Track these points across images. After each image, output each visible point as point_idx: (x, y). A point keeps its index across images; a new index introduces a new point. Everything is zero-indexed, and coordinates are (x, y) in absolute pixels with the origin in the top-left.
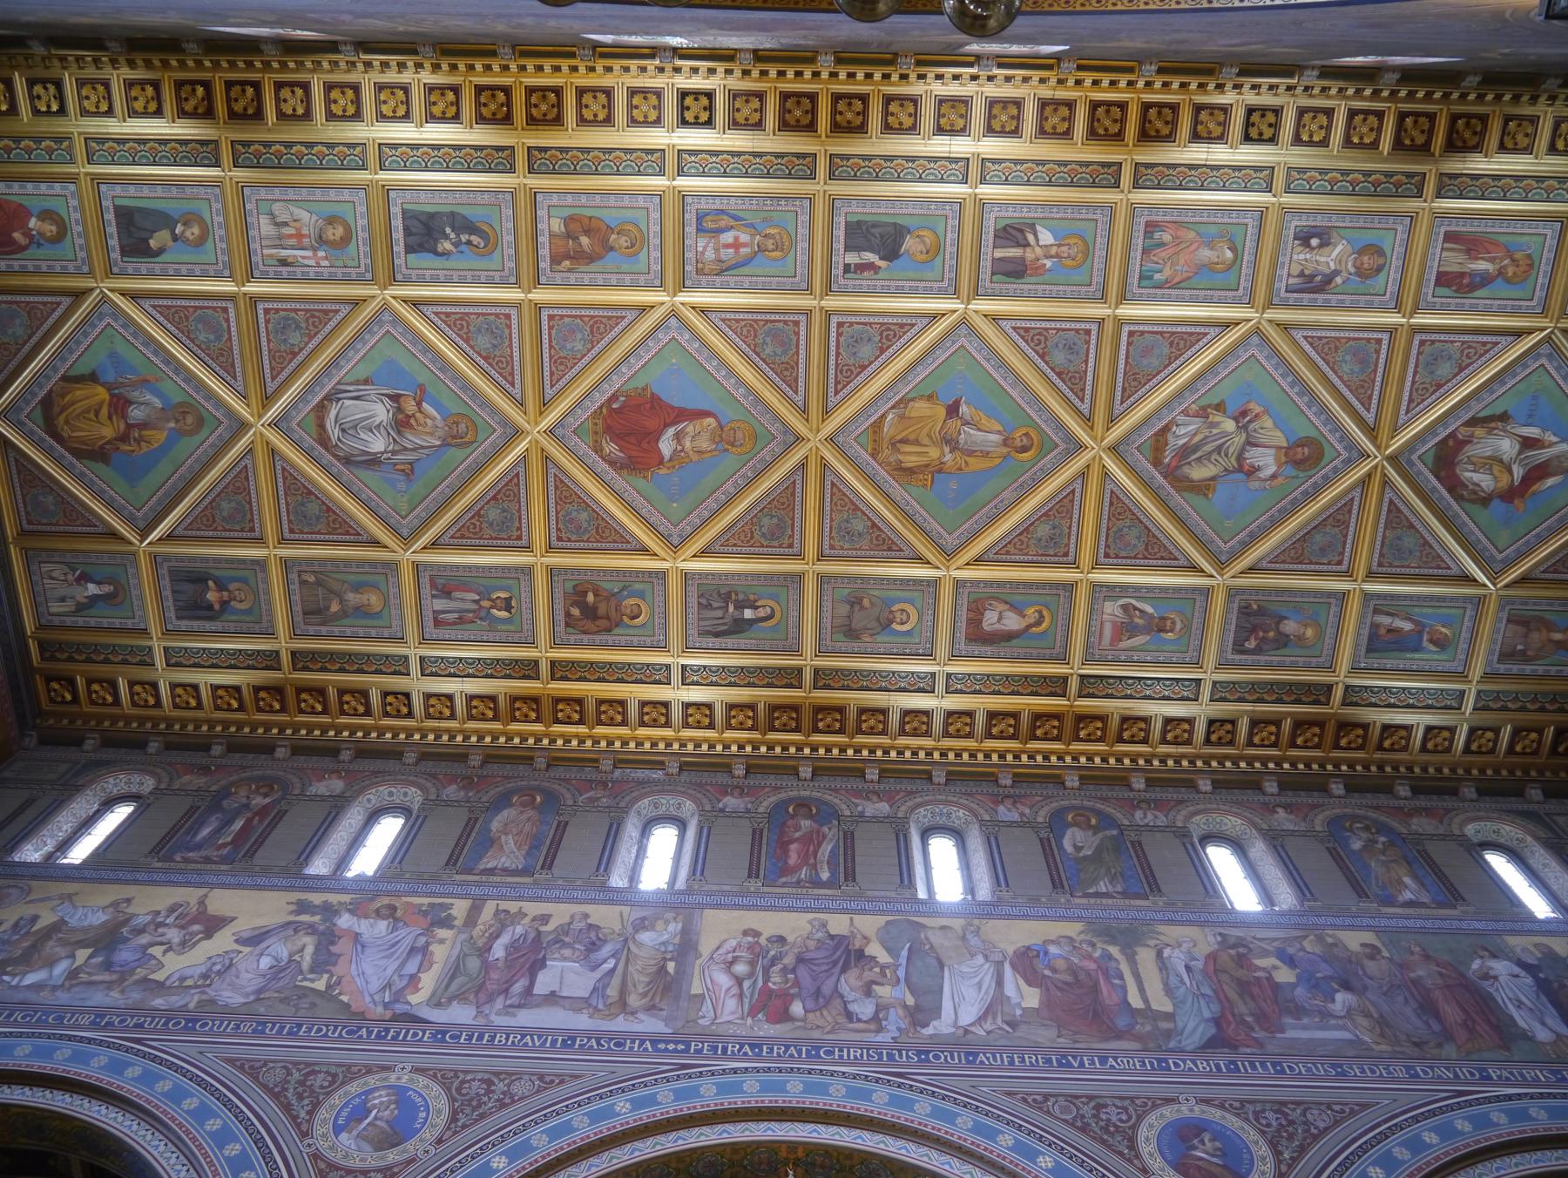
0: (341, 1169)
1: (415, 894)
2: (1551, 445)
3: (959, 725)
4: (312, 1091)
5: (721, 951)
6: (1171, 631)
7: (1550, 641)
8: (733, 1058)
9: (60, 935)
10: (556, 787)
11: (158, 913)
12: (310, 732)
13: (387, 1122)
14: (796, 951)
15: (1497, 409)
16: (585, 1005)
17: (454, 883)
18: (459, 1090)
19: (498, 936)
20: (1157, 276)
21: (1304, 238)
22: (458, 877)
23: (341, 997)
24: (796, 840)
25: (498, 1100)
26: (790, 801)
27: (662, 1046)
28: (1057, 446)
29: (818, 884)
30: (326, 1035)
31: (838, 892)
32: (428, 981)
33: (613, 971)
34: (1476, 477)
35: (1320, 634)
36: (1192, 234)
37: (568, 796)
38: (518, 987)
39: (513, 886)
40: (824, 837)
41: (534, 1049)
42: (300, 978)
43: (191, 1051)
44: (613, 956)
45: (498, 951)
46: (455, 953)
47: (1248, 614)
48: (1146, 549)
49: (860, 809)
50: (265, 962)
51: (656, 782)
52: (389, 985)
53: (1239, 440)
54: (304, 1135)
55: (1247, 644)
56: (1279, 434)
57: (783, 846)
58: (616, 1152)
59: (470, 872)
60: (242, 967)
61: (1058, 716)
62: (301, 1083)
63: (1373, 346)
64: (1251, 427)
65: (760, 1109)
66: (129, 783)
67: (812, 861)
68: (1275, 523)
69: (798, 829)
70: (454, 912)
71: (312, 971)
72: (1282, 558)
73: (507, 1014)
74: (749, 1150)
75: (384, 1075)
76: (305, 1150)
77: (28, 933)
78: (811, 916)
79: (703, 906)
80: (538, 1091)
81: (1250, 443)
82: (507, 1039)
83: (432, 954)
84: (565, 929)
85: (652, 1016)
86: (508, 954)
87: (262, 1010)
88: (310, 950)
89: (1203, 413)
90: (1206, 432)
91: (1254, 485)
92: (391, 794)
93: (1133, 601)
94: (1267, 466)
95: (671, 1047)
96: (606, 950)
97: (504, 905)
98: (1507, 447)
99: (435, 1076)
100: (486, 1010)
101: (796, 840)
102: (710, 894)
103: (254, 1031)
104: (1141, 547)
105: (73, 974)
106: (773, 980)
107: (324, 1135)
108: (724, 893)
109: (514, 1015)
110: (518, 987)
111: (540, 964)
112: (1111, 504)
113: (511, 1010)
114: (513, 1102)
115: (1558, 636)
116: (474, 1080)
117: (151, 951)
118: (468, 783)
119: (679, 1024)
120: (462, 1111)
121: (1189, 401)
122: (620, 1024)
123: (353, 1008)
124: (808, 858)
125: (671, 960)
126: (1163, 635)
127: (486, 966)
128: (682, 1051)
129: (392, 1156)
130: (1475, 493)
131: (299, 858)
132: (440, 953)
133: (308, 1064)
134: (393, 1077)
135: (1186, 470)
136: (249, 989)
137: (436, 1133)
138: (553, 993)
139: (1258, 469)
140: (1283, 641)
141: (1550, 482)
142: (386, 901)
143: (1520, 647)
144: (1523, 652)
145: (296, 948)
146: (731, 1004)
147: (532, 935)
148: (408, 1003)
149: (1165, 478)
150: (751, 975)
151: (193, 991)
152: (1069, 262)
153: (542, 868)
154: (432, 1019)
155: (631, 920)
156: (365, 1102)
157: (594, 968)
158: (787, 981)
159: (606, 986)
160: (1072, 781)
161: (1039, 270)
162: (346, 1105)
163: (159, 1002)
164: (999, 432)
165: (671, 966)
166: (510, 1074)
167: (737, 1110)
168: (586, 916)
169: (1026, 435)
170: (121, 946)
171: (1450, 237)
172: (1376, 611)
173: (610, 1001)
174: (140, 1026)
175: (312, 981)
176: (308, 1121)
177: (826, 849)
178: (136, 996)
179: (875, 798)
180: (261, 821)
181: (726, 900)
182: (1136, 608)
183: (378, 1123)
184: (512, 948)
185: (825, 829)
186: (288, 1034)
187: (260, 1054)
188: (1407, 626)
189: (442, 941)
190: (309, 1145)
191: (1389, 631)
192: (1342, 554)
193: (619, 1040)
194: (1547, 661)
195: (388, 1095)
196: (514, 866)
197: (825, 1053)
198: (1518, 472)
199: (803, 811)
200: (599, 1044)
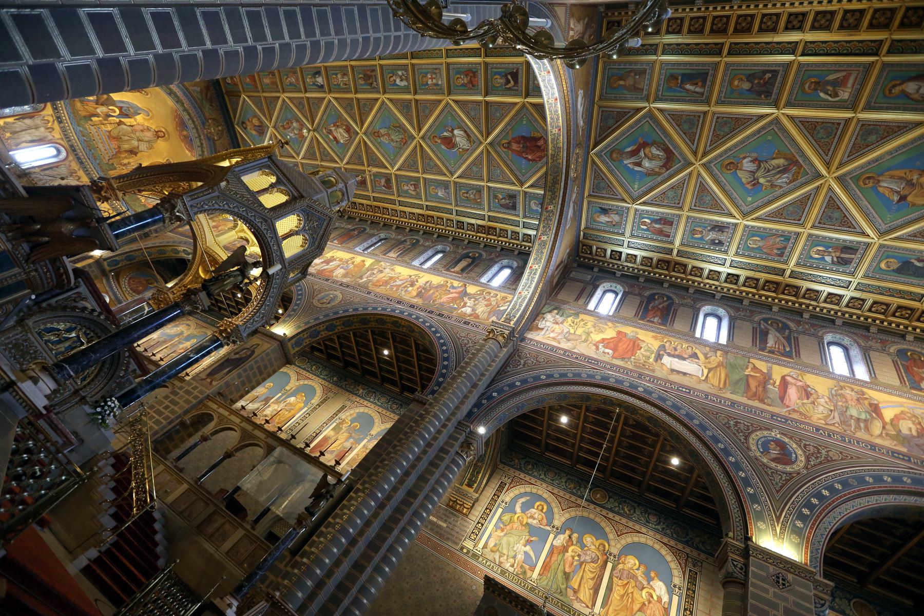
2: (630, 163)
6: (812, 82)
7: (624, 80)
15: (650, 178)
20: (783, 239)
21: (721, 243)
28: (851, 178)
34: (658, 153)
35: (731, 82)
36: (765, 250)
47: (767, 92)
48: (816, 127)
53: (758, 174)
55: (770, 75)
56: (740, 175)
63: (697, 205)
64: (752, 179)
68: (748, 137)
72: (746, 121)
81: (753, 173)
89: (773, 186)
90: (773, 178)
91: (755, 155)
93: (830, 99)
94: (747, 163)
98: (646, 164)
104: (818, 128)
112: (829, 150)
115: (622, 83)
121: (779, 192)
126: (817, 80)
130: (659, 146)
135: (786, 163)
139: (751, 161)
140: (750, 78)
141: (629, 149)
143: (637, 77)
144: (636, 75)
149: (797, 160)
152: (820, 248)
161: (836, 248)
164: (880, 187)
169: (865, 184)
171: (669, 236)
172: (702, 94)
182: (830, 95)
188: (688, 87)
191: (697, 84)
192: (716, 122)
194: (626, 70)
198: (642, 154)
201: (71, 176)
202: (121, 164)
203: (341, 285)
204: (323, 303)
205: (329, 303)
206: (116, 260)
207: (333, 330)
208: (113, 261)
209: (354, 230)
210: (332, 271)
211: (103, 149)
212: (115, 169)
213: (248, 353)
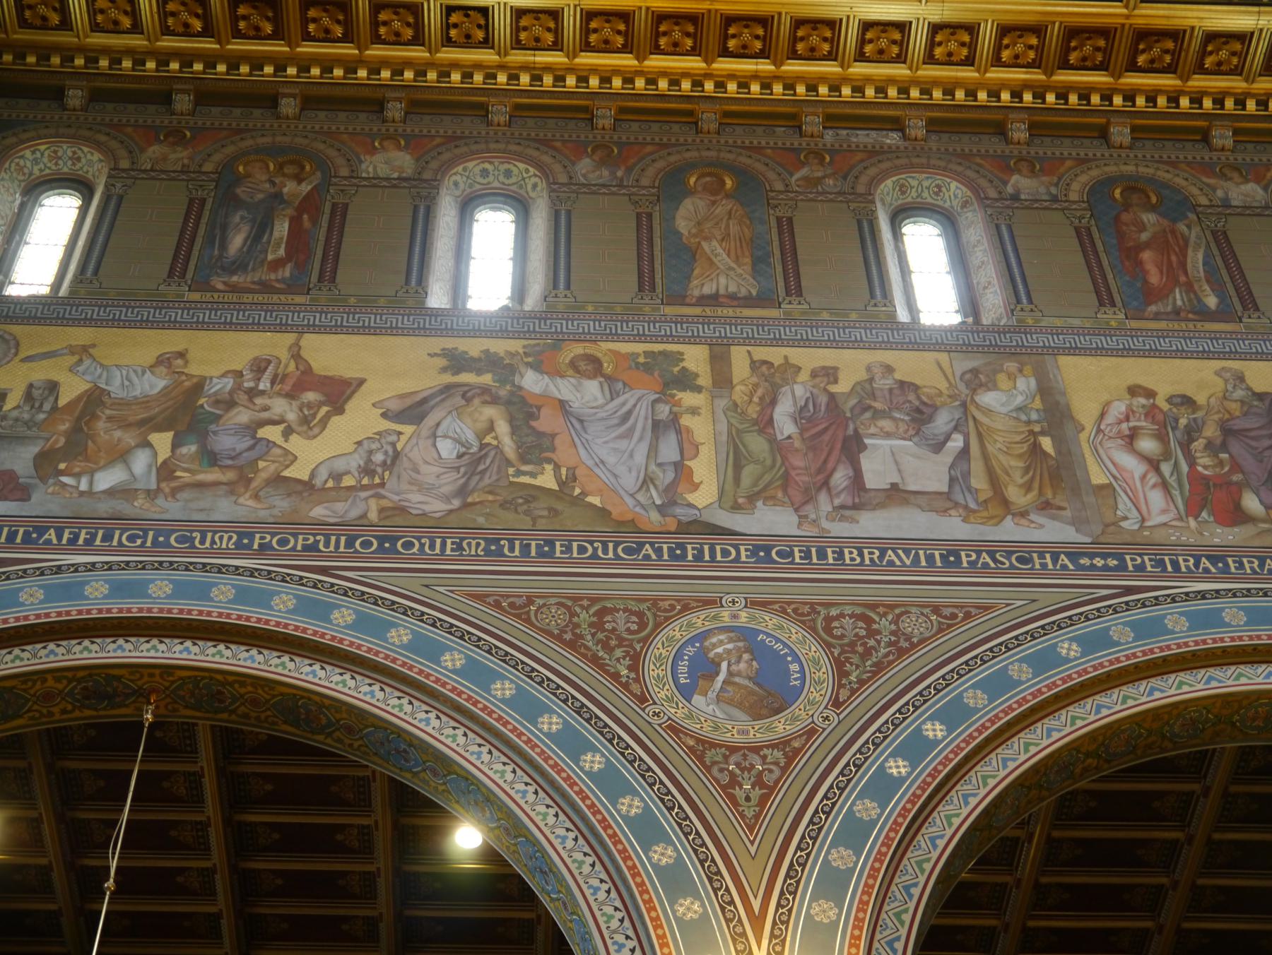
0: (721, 746)
1: (614, 337)
3: (1019, 48)
4: (621, 639)
5: (1110, 419)
8: (1190, 576)
9: (108, 412)
10: (744, 160)
11: (239, 374)
12: (327, 70)
13: (750, 678)
14: (1216, 417)
16: (949, 504)
17: (665, 319)
18: (828, 630)
19: (773, 402)
22: (669, 310)
23: (590, 499)
24: (1147, 245)
25: (890, 644)
26: (1111, 181)
27: (1112, 563)
29: (1205, 314)
30: (595, 556)
31: (774, 313)
32: (704, 468)
33: (965, 452)
37: (771, 175)
38: (841, 477)
39: (761, 323)
40: (1186, 241)
41: (903, 570)
42: (511, 471)
43: (411, 584)
44: (956, 429)
45: (785, 426)
46: (723, 427)
49: (1220, 193)
50: (447, 449)
51: (889, 151)
52: (648, 481)
54: (642, 699)
57: (1131, 253)
58: (1075, 710)
59: (680, 299)
60: (415, 455)
61: (1105, 32)
62: (598, 626)
65: (1255, 647)
66: (56, 157)
67: (1183, 279)
69: (1142, 228)
70: (690, 364)
71: (524, 459)
73: (843, 519)
74: (1245, 703)
75: (713, 612)
76: (655, 721)
77: (55, 408)
78: (1217, 364)
79: (1056, 352)
80: (940, 630)
82: (861, 555)
83: (688, 430)
84: (866, 389)
85: (1053, 518)
86: (802, 431)
87: (481, 520)
88: (503, 428)
92: (485, 173)
95: (1099, 562)
96: (942, 421)
97: (761, 353)
99: (784, 611)
100: (809, 509)
101: (1147, 245)
102: (1055, 331)
103: (239, 545)
105: (166, 471)
106: (1201, 461)
107: (670, 700)
108: (1081, 332)
109: (854, 521)
110: (841, 477)
111: (853, 448)
113: (848, 513)
114: (913, 646)
116: (842, 615)
117: (264, 432)
118: (606, 154)
119: (1098, 529)
120: (847, 659)
122: (1009, 530)
123: (615, 513)
124: (1176, 271)
125: (1043, 433)
127: (779, 448)
128: (1116, 569)
129: (781, 726)
131: (407, 282)
132: (700, 427)
133: (594, 600)
134: (726, 615)
136: (446, 489)
137: (827, 689)
138: (894, 486)
142: (578, 349)
145: (481, 425)
146: (1156, 499)
147: (823, 399)
148: (691, 506)
150: (1167, 455)
151: (363, 494)
153: (320, 280)
154: (738, 529)
155: (958, 374)
156: (703, 652)
157: (938, 447)
158: (1221, 463)
159: (967, 475)
160: (1120, 133)
162: (678, 657)
163: (319, 512)
165: (1047, 443)
166: (891, 607)
167: (1224, 650)
168: (889, 369)
170: (213, 427)
173: (982, 498)
174: (313, 548)
175: (533, 475)
176: (637, 680)
177: (1196, 259)
178: (281, 504)
179: (1235, 175)
180: (315, 221)
181: (1083, 341)
183: (737, 679)
184: (802, 416)
185: (1182, 227)
186: (24, 541)
187: (519, 587)
189: (694, 411)
190: (657, 714)
193: (1023, 554)
195: (731, 640)
196: (743, 292)
197: (778, 553)
199: (1135, 198)
200: (995, 560)
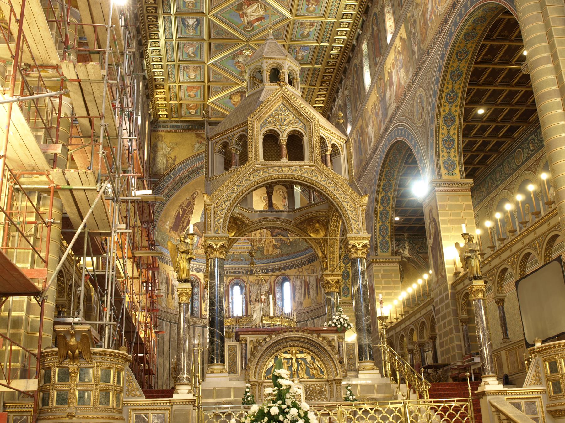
201: (260, 285)
202: (260, 241)
203: (413, 82)
204: (422, 116)
205: (423, 108)
206: (344, 288)
207: (453, 118)
208: (343, 291)
209: (373, 29)
210: (400, 83)
211: (243, 250)
212: (263, 247)
213: (434, 226)
